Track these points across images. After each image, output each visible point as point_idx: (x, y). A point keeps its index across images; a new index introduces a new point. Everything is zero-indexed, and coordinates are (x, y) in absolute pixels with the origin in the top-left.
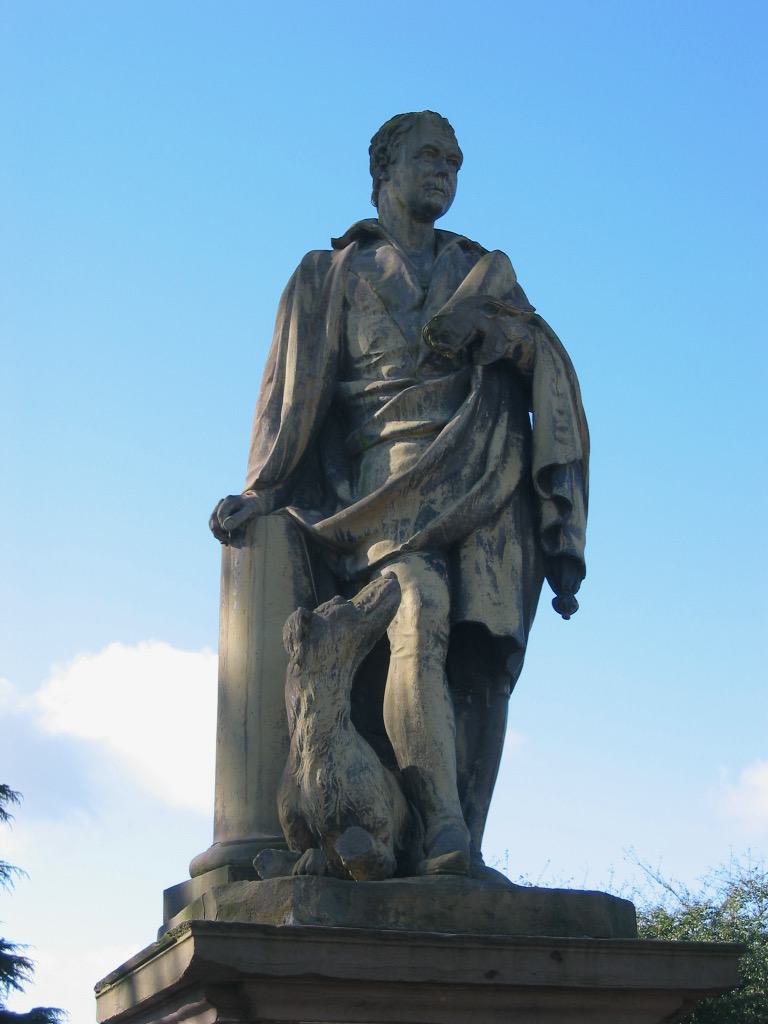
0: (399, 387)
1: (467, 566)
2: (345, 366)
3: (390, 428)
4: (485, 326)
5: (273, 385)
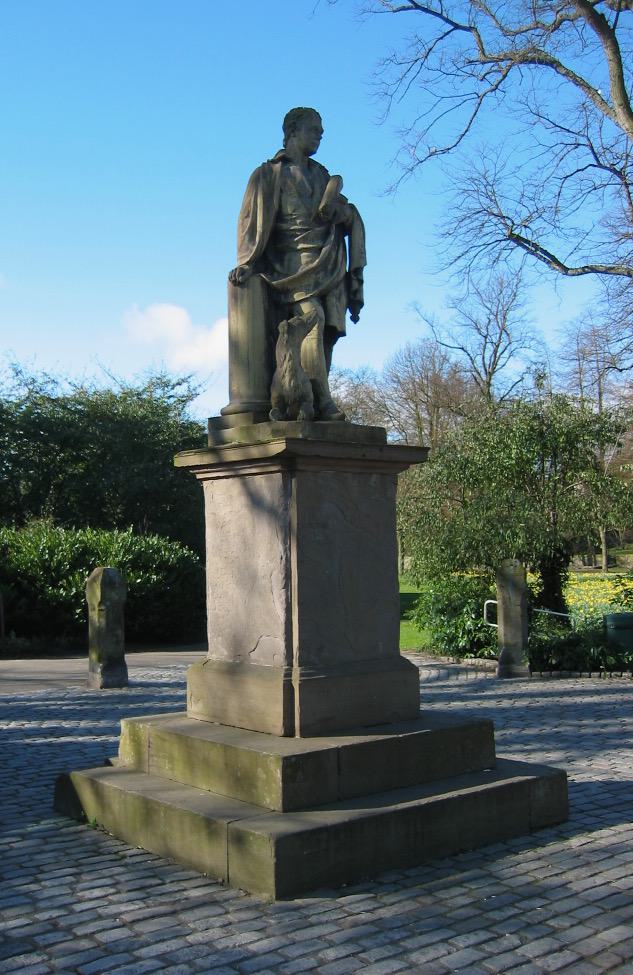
0: (306, 230)
1: (329, 304)
2: (280, 217)
3: (300, 246)
4: (338, 209)
5: (250, 220)
